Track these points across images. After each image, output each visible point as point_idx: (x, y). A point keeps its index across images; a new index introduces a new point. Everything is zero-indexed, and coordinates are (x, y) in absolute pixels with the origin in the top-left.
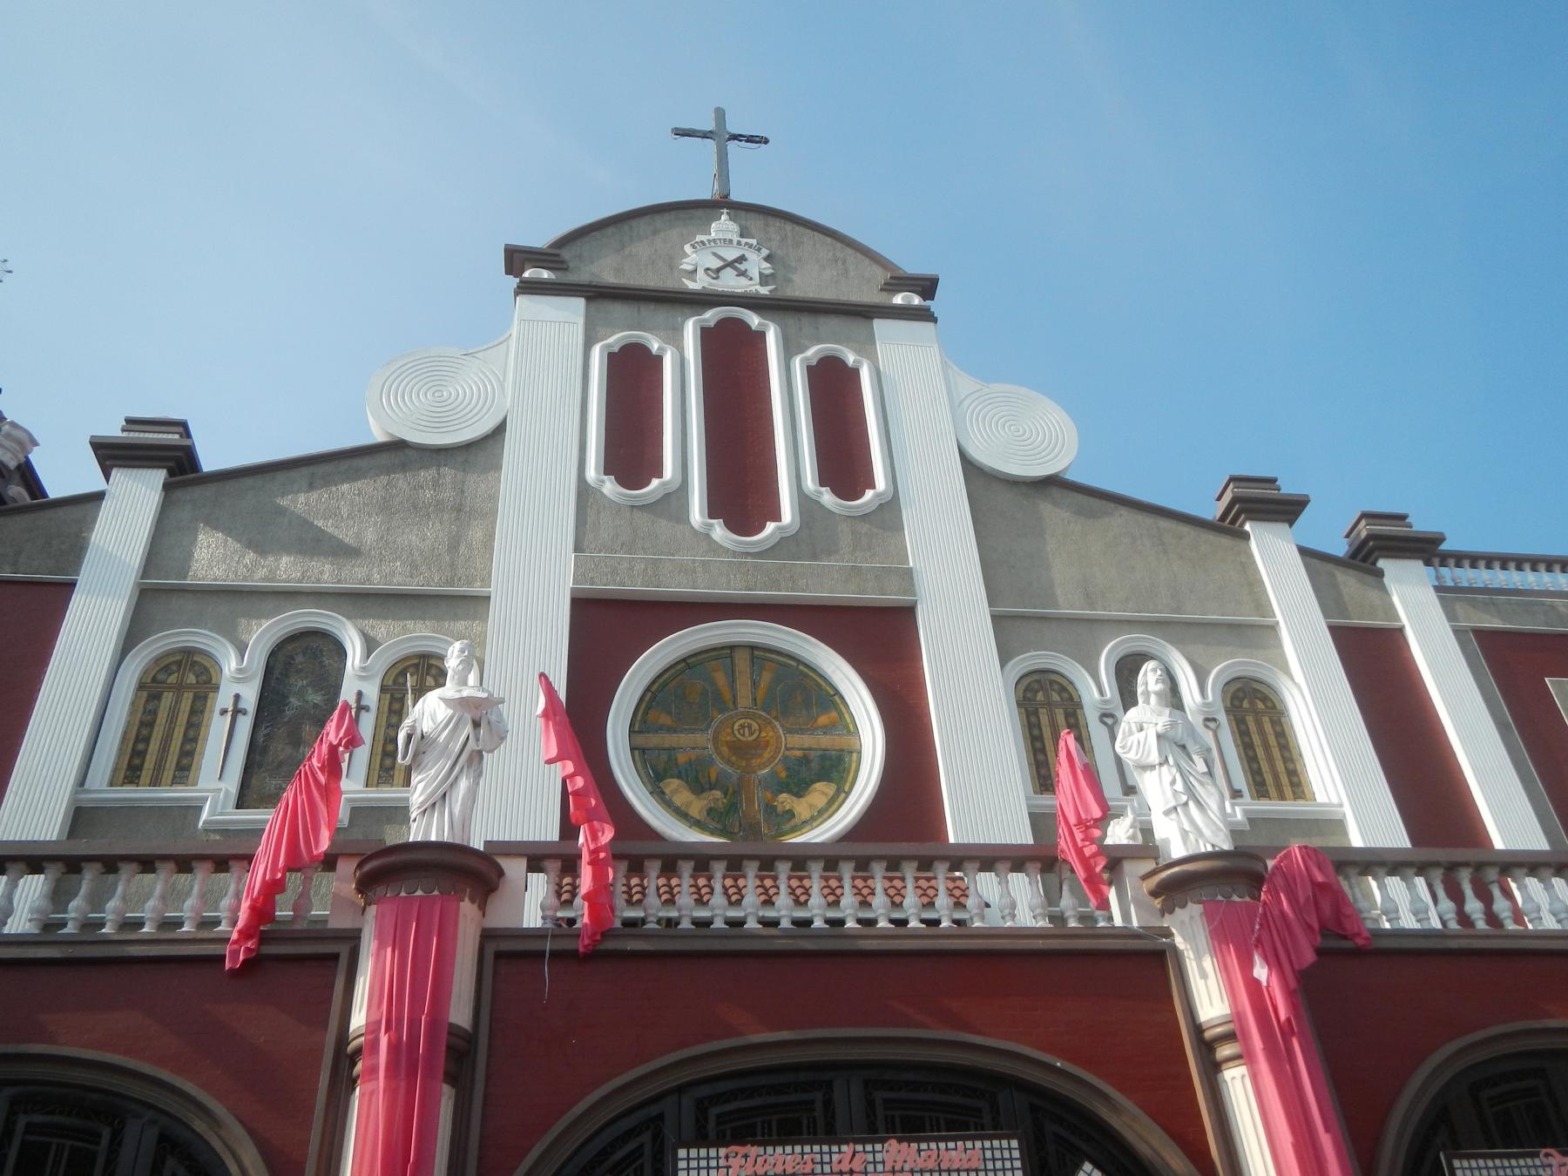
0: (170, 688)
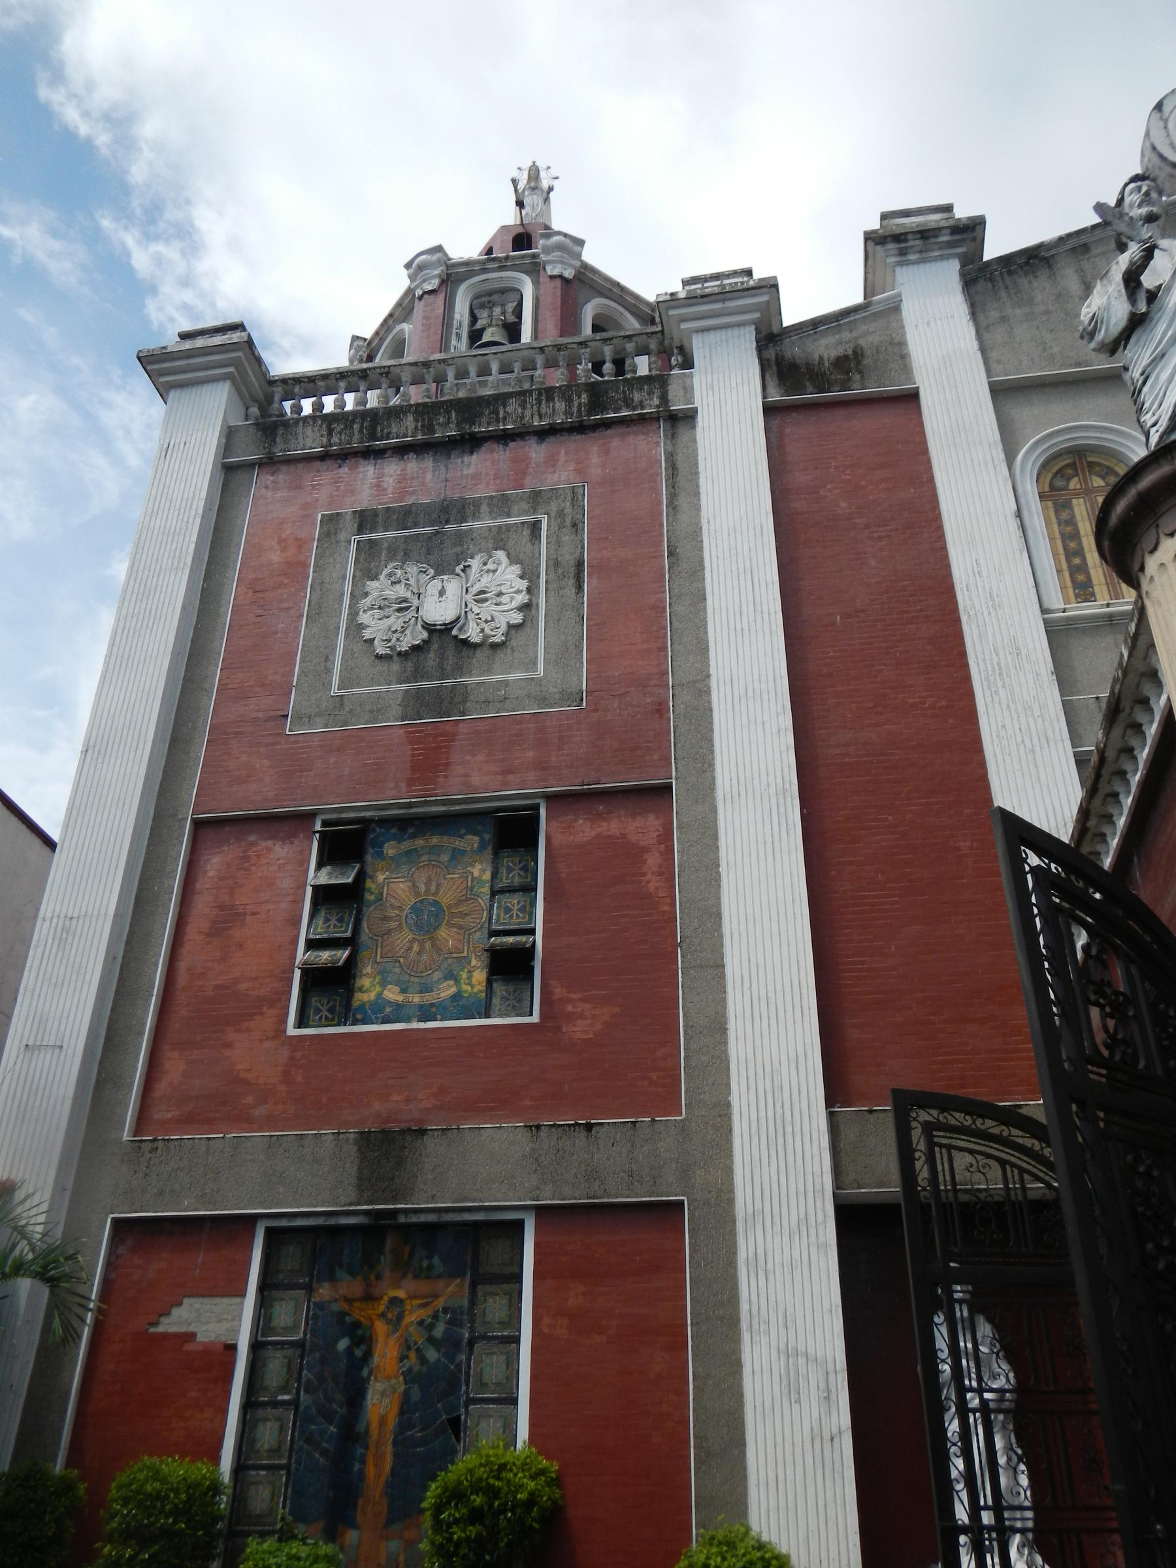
0: (1078, 495)
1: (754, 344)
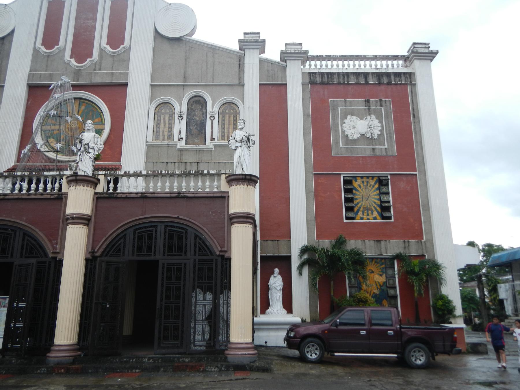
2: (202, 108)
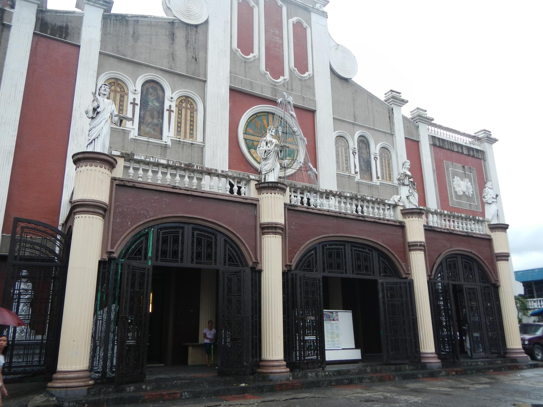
1: (36, 11)
2: (366, 148)
